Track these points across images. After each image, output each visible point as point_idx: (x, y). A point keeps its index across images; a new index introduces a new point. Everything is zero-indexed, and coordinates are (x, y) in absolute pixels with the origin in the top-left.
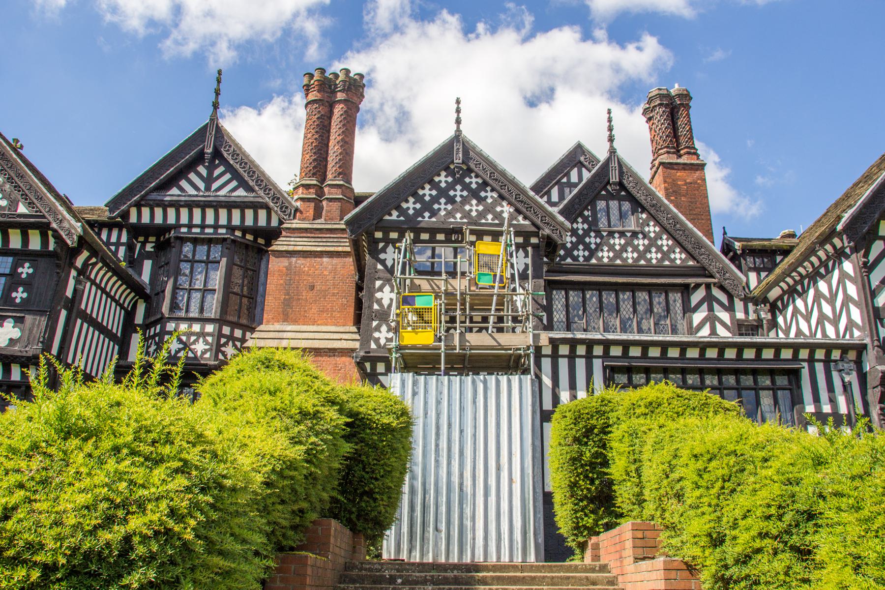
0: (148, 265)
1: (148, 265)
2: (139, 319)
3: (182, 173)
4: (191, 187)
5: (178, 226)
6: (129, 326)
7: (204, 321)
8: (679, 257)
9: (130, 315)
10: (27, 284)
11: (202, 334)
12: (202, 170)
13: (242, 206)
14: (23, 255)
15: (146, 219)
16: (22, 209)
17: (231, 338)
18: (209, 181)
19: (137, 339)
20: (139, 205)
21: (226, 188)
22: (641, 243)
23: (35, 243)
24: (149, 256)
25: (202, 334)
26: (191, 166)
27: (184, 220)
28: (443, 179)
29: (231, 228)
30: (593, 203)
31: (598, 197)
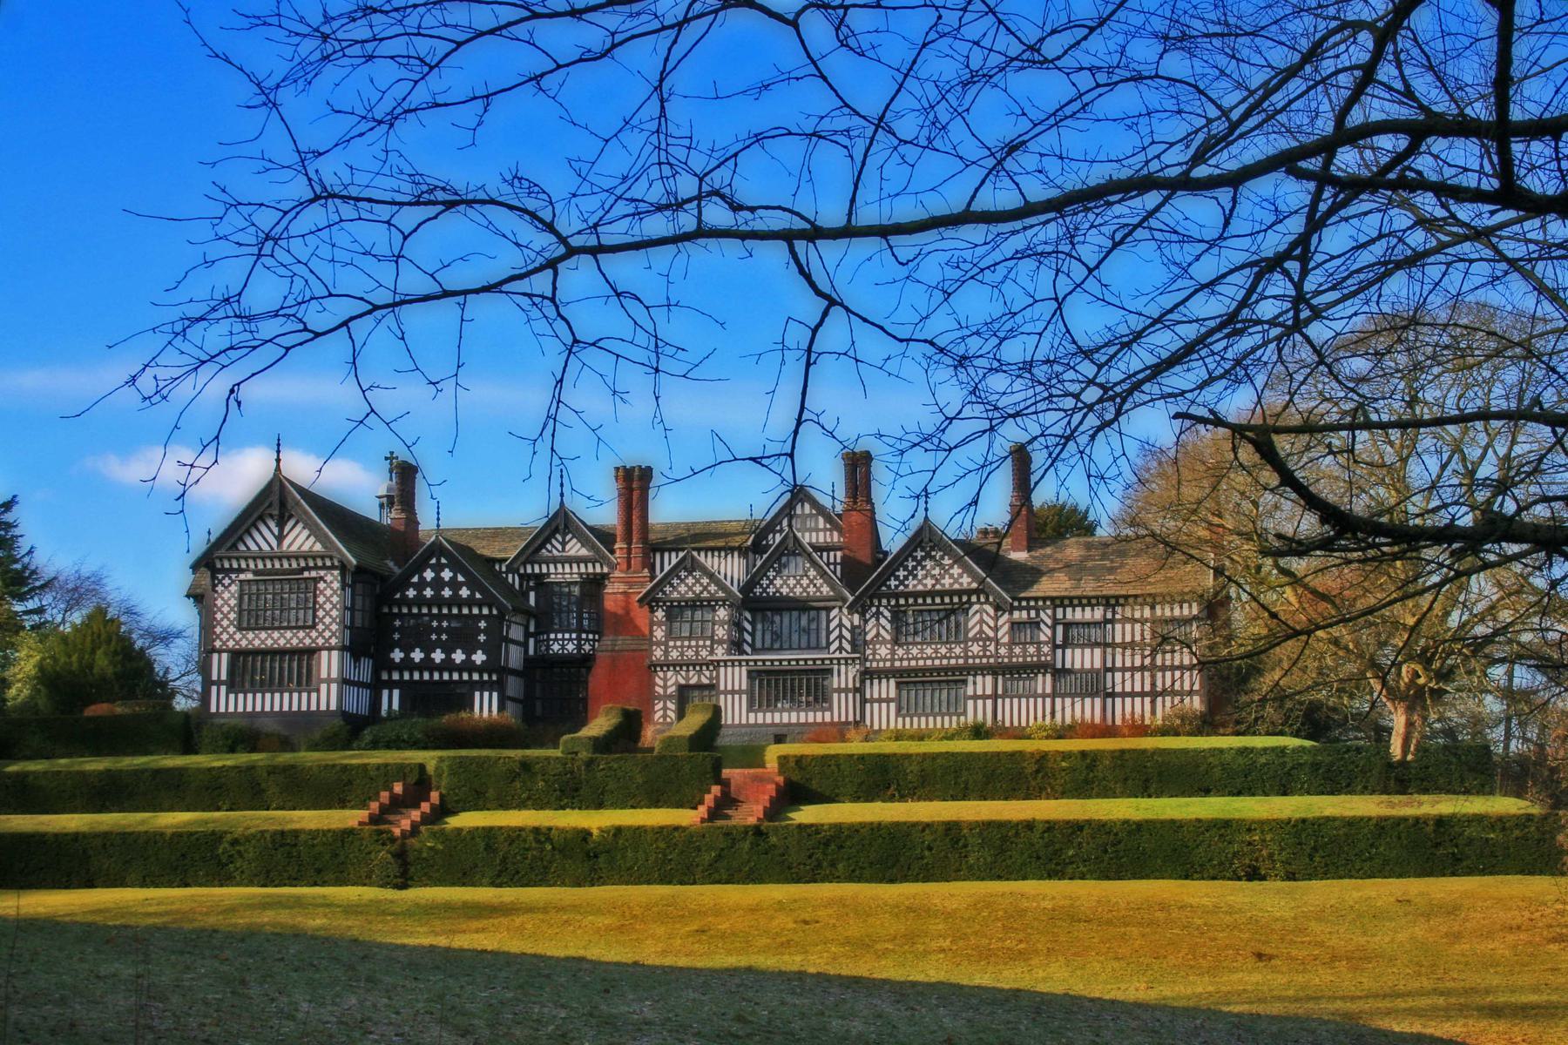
0: (532, 594)
1: (532, 594)
2: (532, 629)
3: (548, 540)
4: (554, 549)
5: (548, 574)
6: (527, 635)
7: (571, 632)
8: (825, 589)
9: (527, 627)
10: (485, 631)
11: (570, 639)
12: (559, 537)
13: (585, 560)
14: (481, 617)
15: (529, 570)
16: (478, 596)
17: (587, 640)
18: (564, 544)
19: (532, 641)
20: (524, 564)
21: (575, 548)
22: (805, 582)
23: (485, 611)
24: (532, 589)
25: (570, 639)
26: (552, 535)
27: (552, 570)
28: (683, 574)
29: (580, 574)
30: (779, 559)
31: (782, 554)
